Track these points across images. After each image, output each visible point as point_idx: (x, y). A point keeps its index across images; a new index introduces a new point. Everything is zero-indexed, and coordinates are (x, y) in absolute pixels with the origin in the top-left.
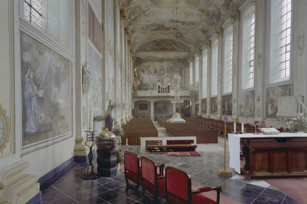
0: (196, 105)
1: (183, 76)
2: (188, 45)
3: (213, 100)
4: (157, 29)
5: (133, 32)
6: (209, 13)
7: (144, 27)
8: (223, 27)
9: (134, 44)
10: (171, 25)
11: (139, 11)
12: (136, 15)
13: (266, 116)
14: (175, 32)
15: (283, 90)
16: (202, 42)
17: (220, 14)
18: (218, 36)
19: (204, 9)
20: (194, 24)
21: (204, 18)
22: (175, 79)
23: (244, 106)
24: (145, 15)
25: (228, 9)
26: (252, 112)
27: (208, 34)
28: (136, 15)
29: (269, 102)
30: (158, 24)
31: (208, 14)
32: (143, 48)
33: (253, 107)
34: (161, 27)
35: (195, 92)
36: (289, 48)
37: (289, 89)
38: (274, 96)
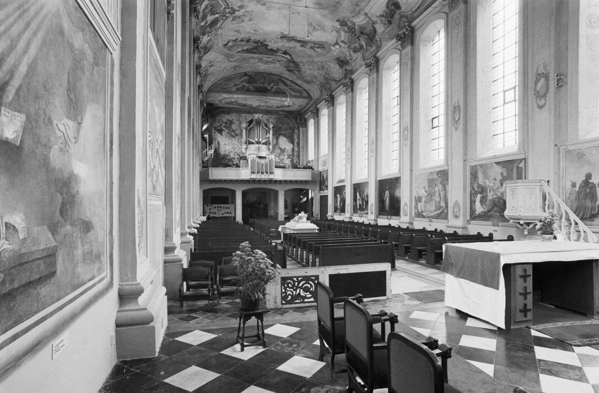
0: (321, 197)
2: (306, 86)
3: (358, 188)
4: (253, 49)
5: (207, 49)
6: (355, 28)
7: (228, 42)
8: (378, 55)
9: (206, 76)
11: (224, 7)
12: (217, 16)
13: (471, 216)
14: (285, 59)
15: (505, 169)
16: (335, 81)
17: (375, 31)
18: (368, 72)
19: (346, 20)
20: (324, 47)
21: (344, 36)
22: (280, 148)
23: (423, 199)
24: (234, 19)
25: (390, 23)
26: (441, 211)
27: (349, 68)
28: (217, 16)
29: (476, 192)
30: (255, 40)
31: (353, 30)
32: (221, 86)
33: (442, 200)
34: (260, 47)
35: (321, 173)
36: (510, 95)
37: (518, 167)
38: (487, 181)
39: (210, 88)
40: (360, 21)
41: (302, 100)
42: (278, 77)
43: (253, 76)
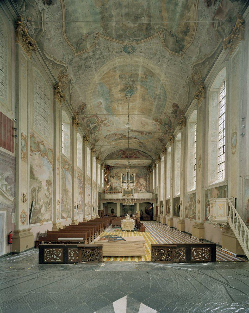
1: (147, 181)
5: (96, 140)
7: (106, 136)
10: (131, 135)
11: (97, 120)
12: (95, 124)
14: (136, 141)
16: (160, 149)
21: (158, 127)
22: (140, 184)
24: (105, 125)
27: (164, 142)
28: (95, 124)
31: (161, 123)
32: (111, 156)
34: (122, 137)
39: (105, 158)
40: (163, 117)
41: (148, 160)
42: (137, 150)
43: (124, 151)
